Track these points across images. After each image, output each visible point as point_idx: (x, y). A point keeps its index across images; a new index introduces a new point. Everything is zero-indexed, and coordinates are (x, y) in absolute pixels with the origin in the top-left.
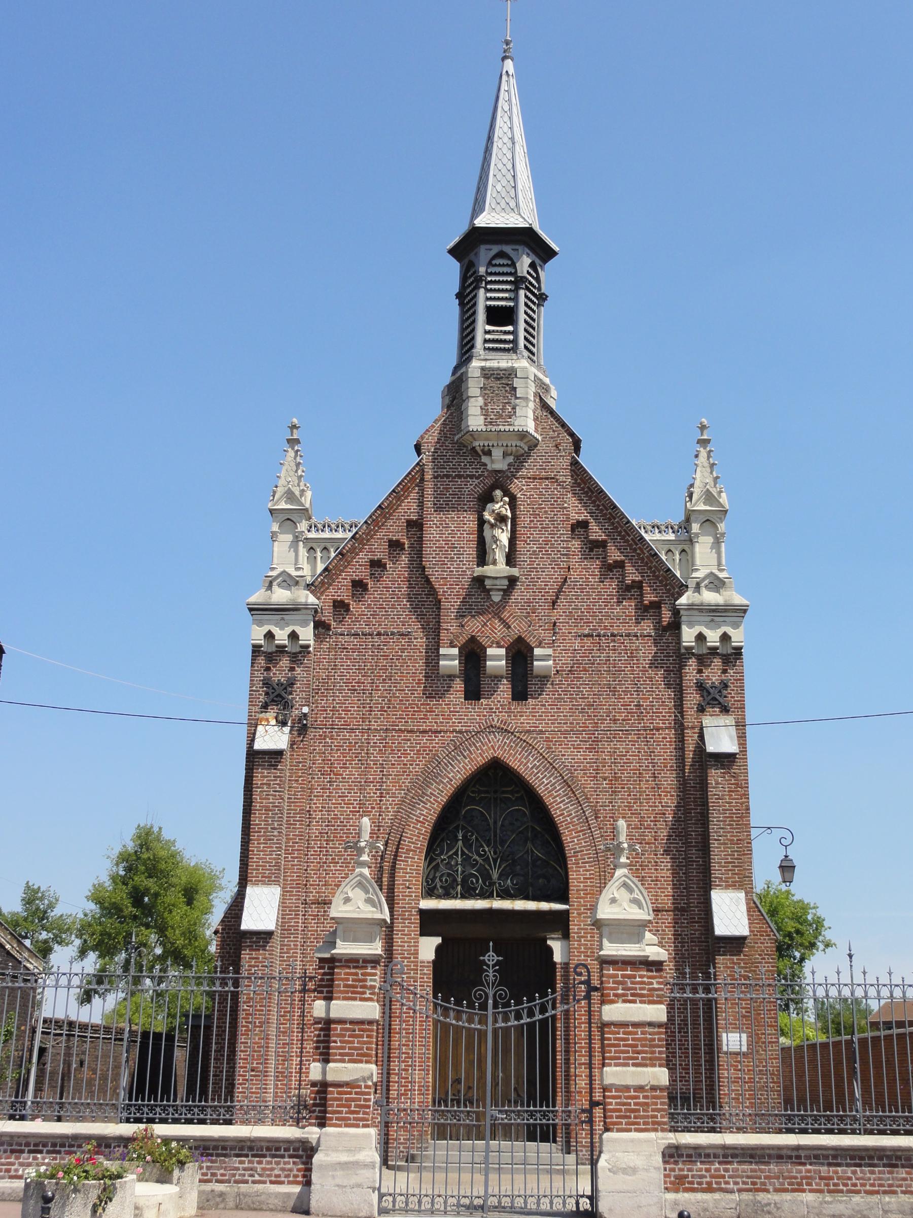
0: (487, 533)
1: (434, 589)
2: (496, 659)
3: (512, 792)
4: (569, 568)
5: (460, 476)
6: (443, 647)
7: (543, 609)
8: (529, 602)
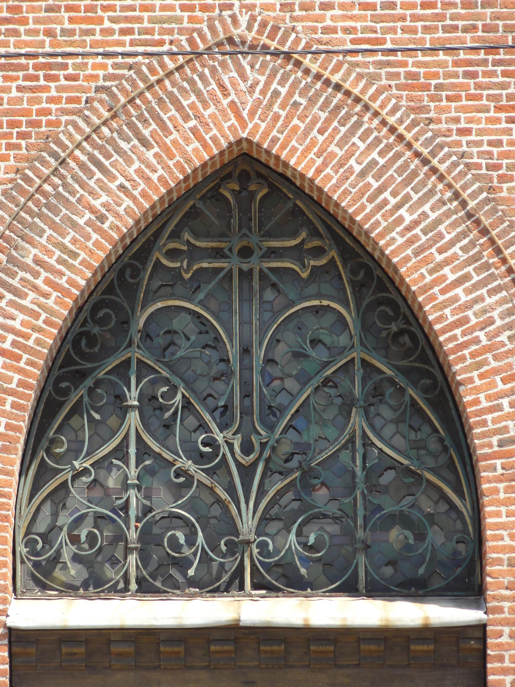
3: (298, 253)
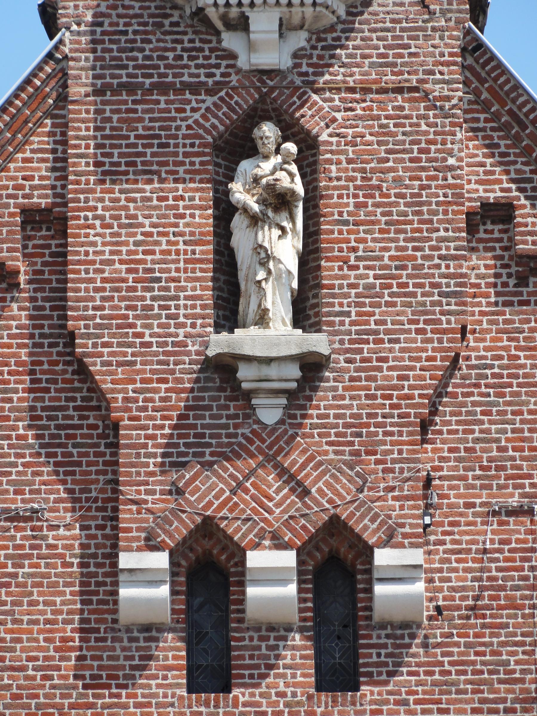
0: (241, 238)
1: (101, 395)
2: (272, 579)
4: (463, 330)
5: (163, 88)
6: (129, 549)
7: (395, 442)
8: (357, 425)
